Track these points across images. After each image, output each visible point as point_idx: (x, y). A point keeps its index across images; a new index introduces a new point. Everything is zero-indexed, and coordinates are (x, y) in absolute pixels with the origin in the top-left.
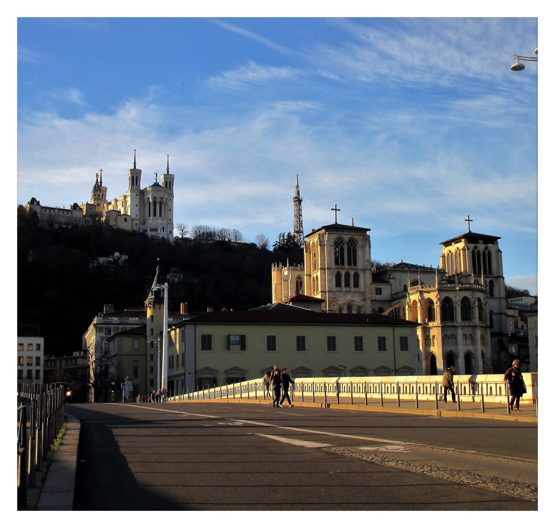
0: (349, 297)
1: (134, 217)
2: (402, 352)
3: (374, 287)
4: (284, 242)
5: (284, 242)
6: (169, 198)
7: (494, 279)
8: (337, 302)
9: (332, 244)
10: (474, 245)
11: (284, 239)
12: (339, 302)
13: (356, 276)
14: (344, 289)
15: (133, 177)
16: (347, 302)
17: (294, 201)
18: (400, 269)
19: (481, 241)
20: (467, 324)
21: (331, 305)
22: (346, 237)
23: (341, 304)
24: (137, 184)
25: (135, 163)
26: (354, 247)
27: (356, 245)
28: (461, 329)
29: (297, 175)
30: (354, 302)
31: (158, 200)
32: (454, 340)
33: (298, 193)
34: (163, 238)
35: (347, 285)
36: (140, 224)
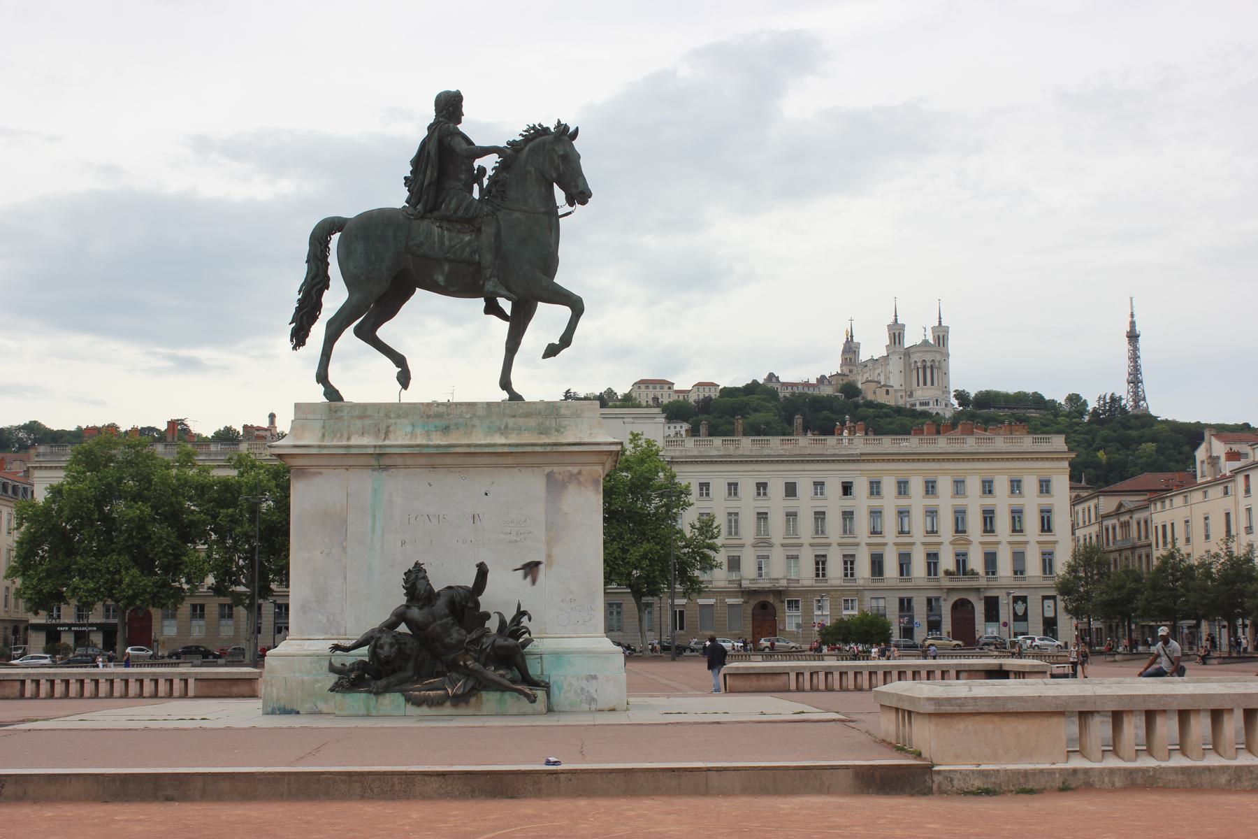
1: (897, 387)
4: (1105, 406)
15: (894, 334)
17: (1128, 337)
24: (899, 343)
29: (1131, 298)
31: (929, 364)
33: (1133, 324)
34: (937, 414)
36: (906, 396)
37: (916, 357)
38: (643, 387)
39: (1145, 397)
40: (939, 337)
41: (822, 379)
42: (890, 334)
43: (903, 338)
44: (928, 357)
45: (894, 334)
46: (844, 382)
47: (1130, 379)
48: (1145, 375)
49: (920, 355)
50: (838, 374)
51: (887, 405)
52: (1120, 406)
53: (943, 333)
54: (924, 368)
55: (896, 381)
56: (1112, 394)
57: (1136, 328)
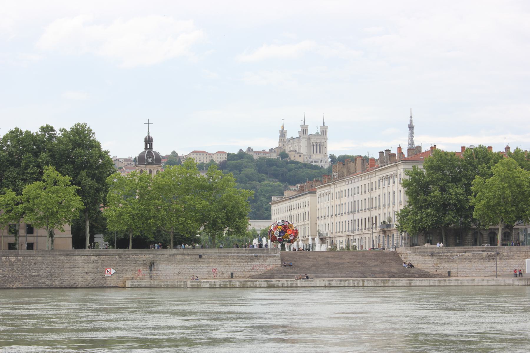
1: (304, 153)
15: (304, 130)
24: (306, 134)
29: (411, 109)
31: (318, 144)
33: (411, 121)
37: (313, 141)
38: (195, 154)
40: (323, 131)
41: (271, 150)
44: (318, 141)
45: (304, 130)
46: (281, 151)
50: (278, 147)
51: (300, 162)
53: (325, 129)
54: (317, 145)
55: (304, 151)
57: (413, 123)
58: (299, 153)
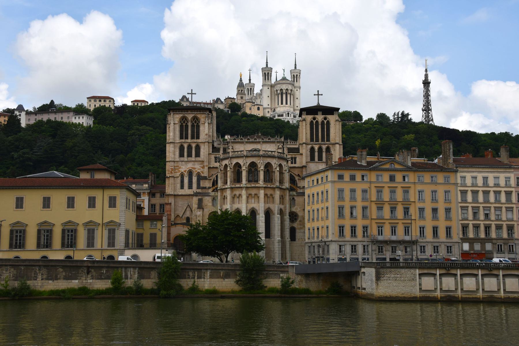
0: (190, 166)
1: (265, 105)
2: (111, 209)
3: (213, 157)
4: (398, 119)
5: (398, 119)
6: (296, 89)
7: (331, 146)
8: (179, 169)
9: (176, 122)
10: (312, 116)
11: (398, 118)
12: (180, 170)
13: (198, 148)
14: (185, 158)
15: (265, 73)
16: (188, 169)
17: (423, 83)
18: (246, 140)
19: (320, 113)
20: (253, 185)
21: (173, 172)
22: (190, 116)
23: (183, 171)
24: (268, 79)
25: (267, 63)
26: (198, 124)
27: (199, 122)
28: (244, 189)
30: (195, 169)
31: (284, 91)
32: (271, 199)
33: (426, 76)
34: (288, 122)
35: (190, 155)
39: (433, 119)
42: (263, 74)
43: (271, 76)
44: (284, 87)
45: (265, 73)
47: (424, 108)
48: (434, 106)
49: (279, 86)
52: (408, 119)
53: (296, 74)
56: (403, 112)
58: (257, 105)
